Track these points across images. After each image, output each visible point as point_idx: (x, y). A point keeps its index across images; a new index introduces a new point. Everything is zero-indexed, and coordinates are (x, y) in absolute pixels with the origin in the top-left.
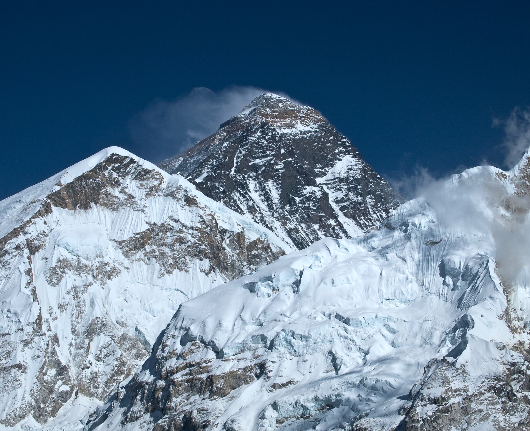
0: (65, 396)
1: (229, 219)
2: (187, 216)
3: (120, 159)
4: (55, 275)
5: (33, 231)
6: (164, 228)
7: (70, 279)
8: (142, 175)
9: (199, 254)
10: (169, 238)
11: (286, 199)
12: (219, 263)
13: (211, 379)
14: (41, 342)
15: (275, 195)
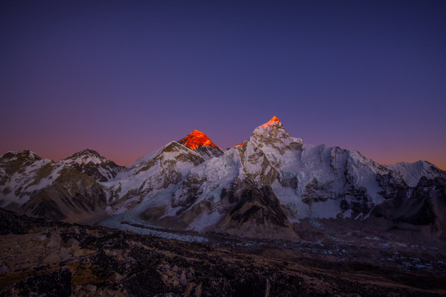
0: (168, 184)
1: (194, 152)
2: (186, 153)
3: (174, 143)
4: (165, 163)
5: (161, 155)
6: (183, 154)
7: (167, 164)
8: (178, 146)
9: (189, 159)
10: (183, 156)
11: (199, 148)
12: (192, 160)
13: (197, 181)
14: (164, 175)
15: (197, 147)
